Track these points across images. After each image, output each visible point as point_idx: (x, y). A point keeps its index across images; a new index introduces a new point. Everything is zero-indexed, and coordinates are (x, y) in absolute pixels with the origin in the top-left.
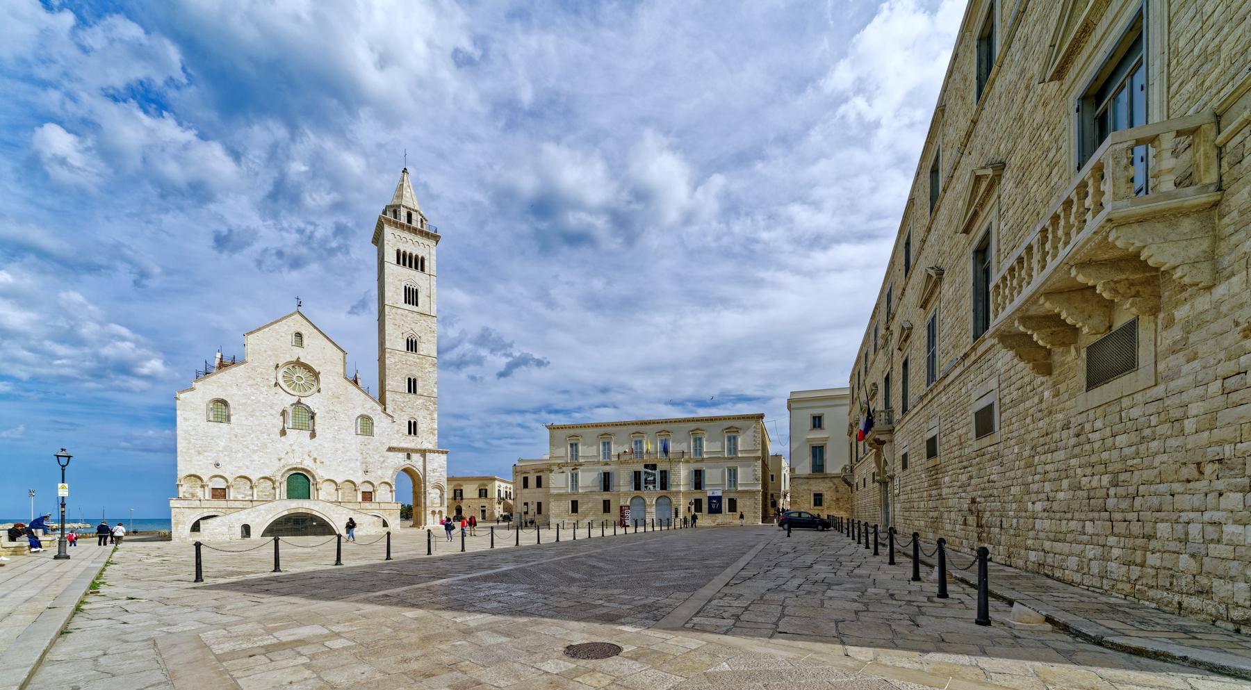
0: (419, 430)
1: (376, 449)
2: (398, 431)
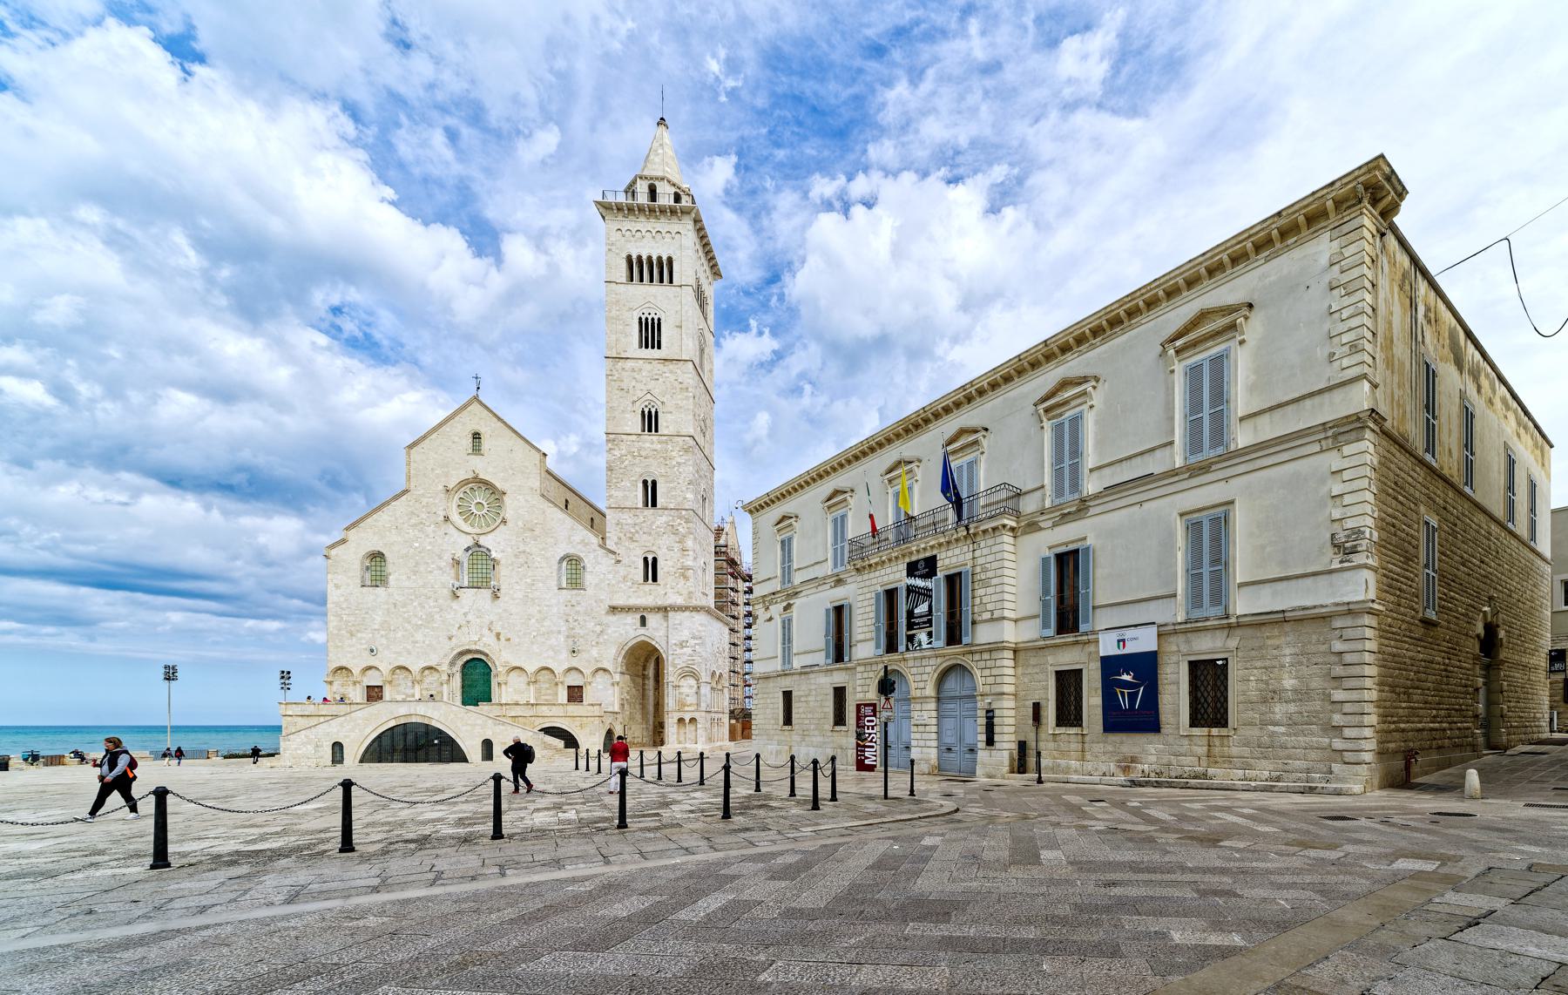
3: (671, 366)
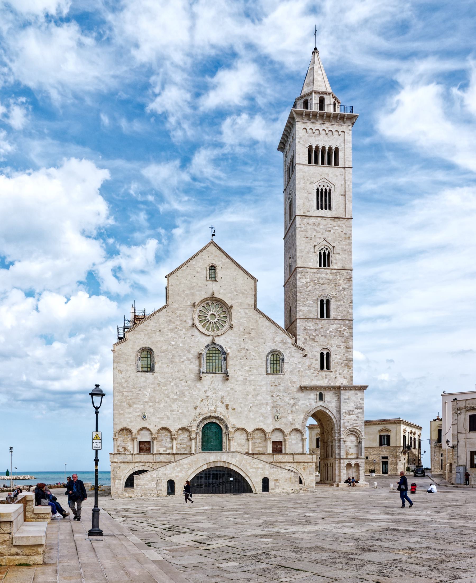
0: (332, 364)
1: (286, 390)
2: (309, 366)
3: (339, 222)
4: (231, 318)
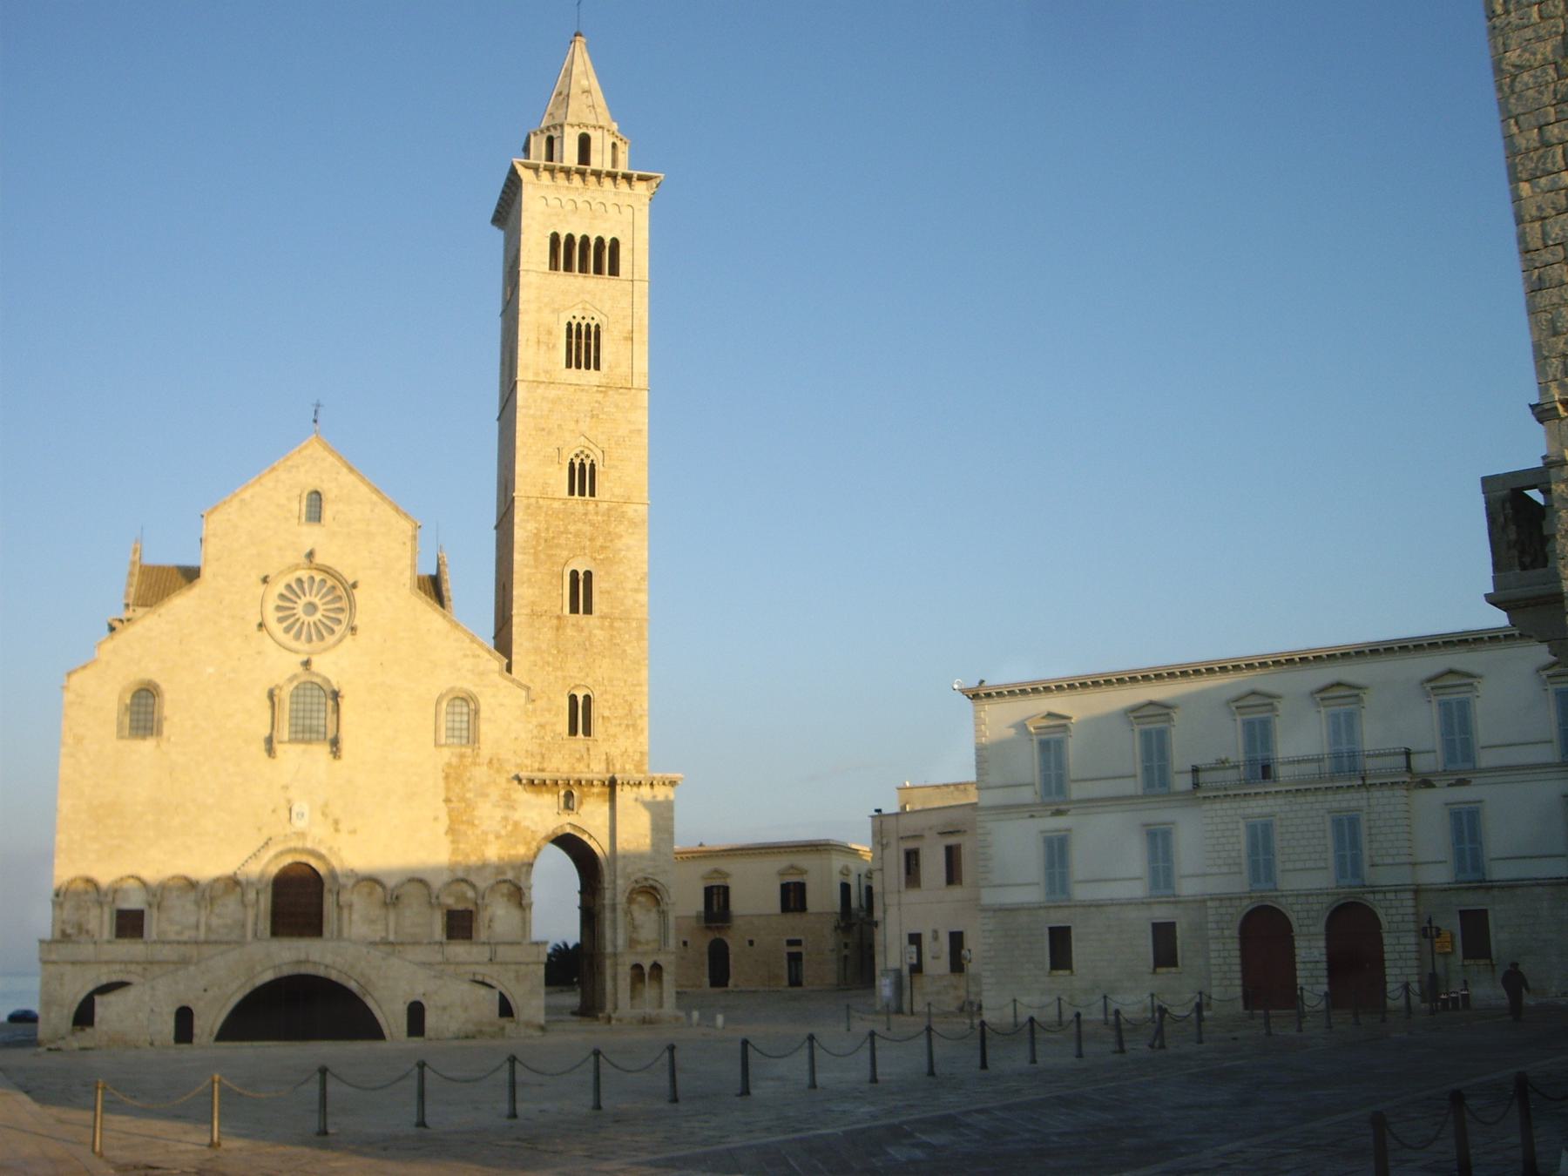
4: (352, 615)
